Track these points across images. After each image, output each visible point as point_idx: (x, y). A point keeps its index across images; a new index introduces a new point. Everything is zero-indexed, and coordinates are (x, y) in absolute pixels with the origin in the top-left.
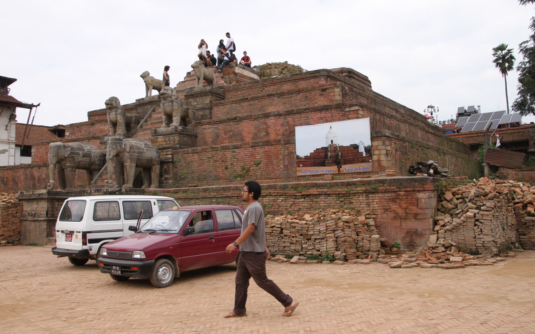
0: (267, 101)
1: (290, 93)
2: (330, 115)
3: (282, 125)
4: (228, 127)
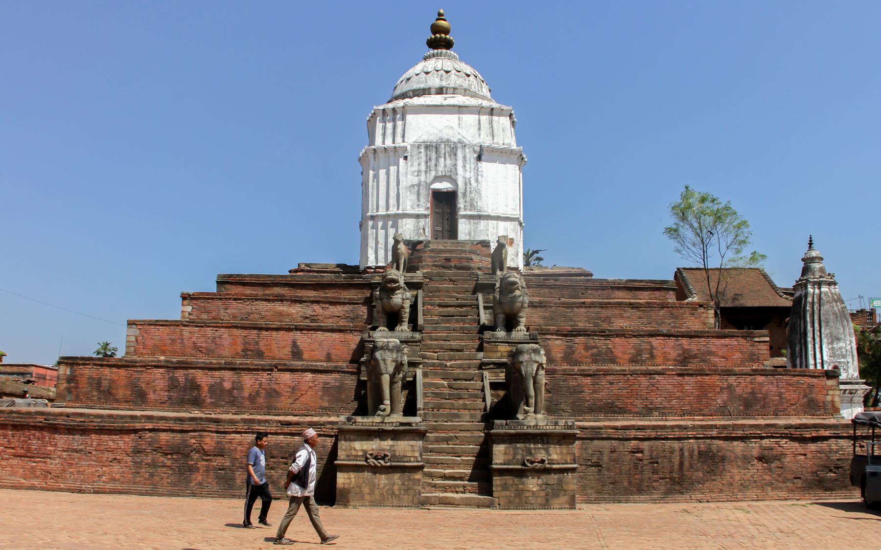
0: (617, 312)
3: (673, 348)
4: (591, 341)
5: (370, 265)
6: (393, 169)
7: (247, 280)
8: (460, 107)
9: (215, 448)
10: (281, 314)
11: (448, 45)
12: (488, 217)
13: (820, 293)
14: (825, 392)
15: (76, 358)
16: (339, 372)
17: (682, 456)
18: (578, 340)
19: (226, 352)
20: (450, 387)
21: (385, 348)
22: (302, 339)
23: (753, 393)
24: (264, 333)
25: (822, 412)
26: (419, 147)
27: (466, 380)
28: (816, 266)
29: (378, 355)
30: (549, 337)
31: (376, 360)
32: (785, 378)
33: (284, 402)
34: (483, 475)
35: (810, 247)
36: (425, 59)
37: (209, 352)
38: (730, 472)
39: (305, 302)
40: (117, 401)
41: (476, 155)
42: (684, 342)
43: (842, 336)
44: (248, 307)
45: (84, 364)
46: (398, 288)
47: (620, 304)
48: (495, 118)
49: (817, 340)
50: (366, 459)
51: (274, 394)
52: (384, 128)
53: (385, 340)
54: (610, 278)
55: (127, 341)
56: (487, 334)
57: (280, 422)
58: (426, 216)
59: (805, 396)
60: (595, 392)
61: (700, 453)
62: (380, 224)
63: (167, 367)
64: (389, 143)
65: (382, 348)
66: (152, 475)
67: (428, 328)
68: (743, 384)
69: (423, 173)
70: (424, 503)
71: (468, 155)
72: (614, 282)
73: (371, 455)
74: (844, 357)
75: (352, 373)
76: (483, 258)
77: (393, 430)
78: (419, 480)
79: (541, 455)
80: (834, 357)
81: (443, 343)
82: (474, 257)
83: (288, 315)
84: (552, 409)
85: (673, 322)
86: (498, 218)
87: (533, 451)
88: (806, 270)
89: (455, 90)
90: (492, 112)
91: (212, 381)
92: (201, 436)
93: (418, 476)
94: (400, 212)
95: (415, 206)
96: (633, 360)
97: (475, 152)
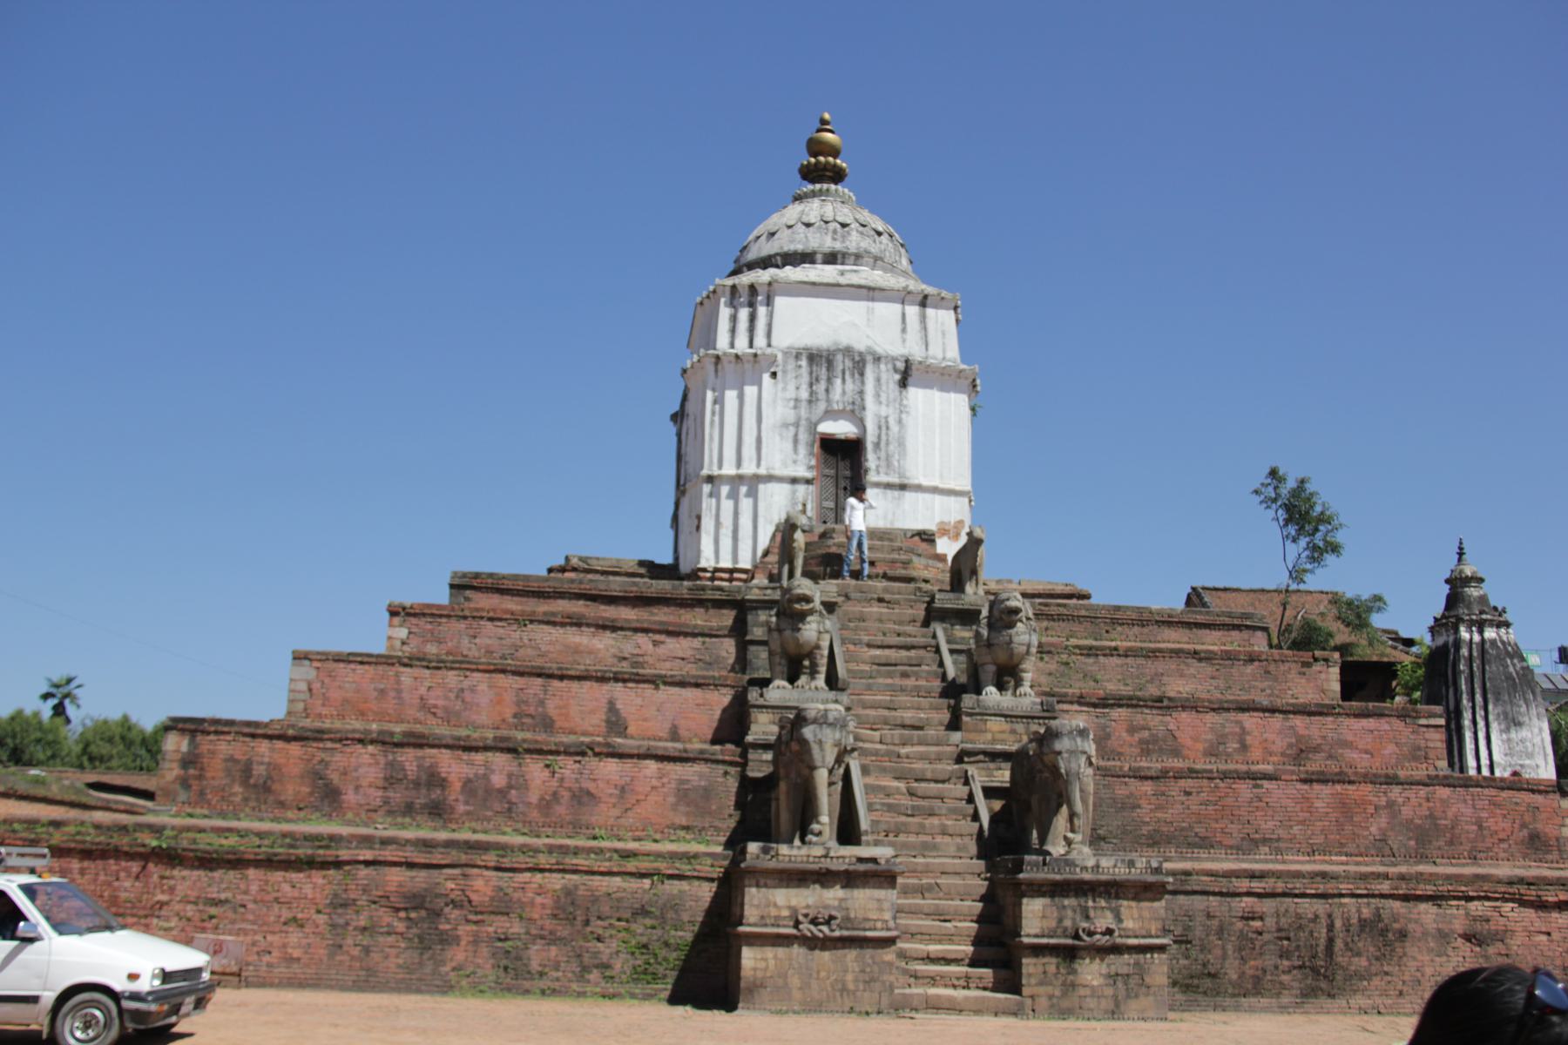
0: (1172, 665)
1: (1229, 657)
2: (1387, 727)
3: (1280, 733)
5: (703, 564)
6: (751, 391)
7: (508, 584)
8: (870, 289)
9: (492, 899)
10: (577, 650)
11: (837, 176)
12: (919, 488)
13: (1483, 640)
14: (1558, 820)
15: (202, 721)
16: (706, 760)
17: (1331, 927)
18: (1116, 713)
19: (483, 718)
20: (911, 793)
21: (822, 720)
22: (628, 698)
23: (1432, 816)
24: (556, 683)
25: (1555, 855)
26: (798, 356)
27: (936, 781)
28: (1473, 592)
29: (808, 732)
30: (1066, 707)
31: (804, 743)
32: (1486, 791)
33: (603, 814)
34: (999, 952)
35: (1460, 560)
36: (798, 198)
37: (449, 717)
38: (1414, 959)
39: (622, 629)
40: (282, 805)
41: (898, 377)
43: (1526, 719)
44: (515, 635)
45: (216, 732)
46: (811, 612)
47: (1177, 653)
48: (930, 312)
49: (1481, 724)
50: (797, 924)
51: (585, 799)
52: (734, 319)
53: (821, 707)
54: (1155, 606)
55: (292, 691)
56: (968, 700)
57: (616, 851)
58: (808, 482)
59: (1523, 826)
60: (1159, 808)
61: (1363, 923)
62: (725, 490)
63: (384, 743)
64: (742, 344)
65: (815, 721)
66: (367, 950)
67: (857, 684)
68: (1413, 800)
69: (804, 404)
70: (900, 1007)
71: (884, 377)
72: (1159, 612)
73: (806, 916)
74: (1530, 756)
75: (731, 763)
76: (931, 562)
77: (846, 872)
78: (890, 964)
79: (1104, 921)
80: (1512, 755)
81: (886, 713)
82: (915, 559)
83: (590, 653)
84: (1096, 840)
85: (1270, 687)
86: (935, 490)
87: (1092, 913)
88: (1453, 600)
89: (858, 258)
90: (924, 302)
91: (469, 771)
92: (465, 875)
93: (888, 955)
94: (762, 471)
95: (789, 462)
96: (1212, 753)
97: (896, 370)
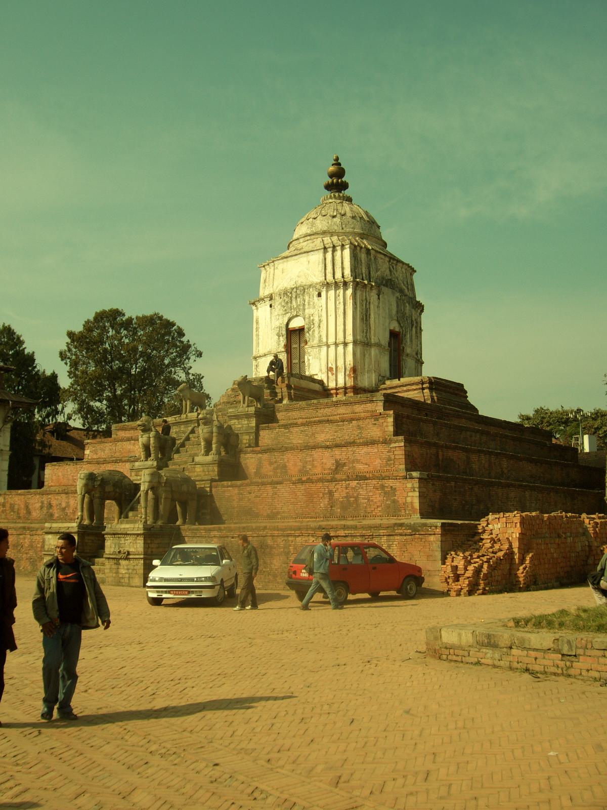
0: (318, 428)
42: (337, 452)
